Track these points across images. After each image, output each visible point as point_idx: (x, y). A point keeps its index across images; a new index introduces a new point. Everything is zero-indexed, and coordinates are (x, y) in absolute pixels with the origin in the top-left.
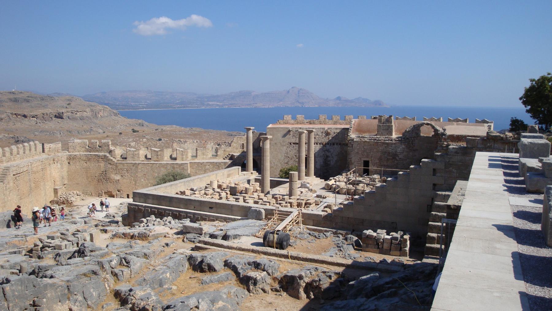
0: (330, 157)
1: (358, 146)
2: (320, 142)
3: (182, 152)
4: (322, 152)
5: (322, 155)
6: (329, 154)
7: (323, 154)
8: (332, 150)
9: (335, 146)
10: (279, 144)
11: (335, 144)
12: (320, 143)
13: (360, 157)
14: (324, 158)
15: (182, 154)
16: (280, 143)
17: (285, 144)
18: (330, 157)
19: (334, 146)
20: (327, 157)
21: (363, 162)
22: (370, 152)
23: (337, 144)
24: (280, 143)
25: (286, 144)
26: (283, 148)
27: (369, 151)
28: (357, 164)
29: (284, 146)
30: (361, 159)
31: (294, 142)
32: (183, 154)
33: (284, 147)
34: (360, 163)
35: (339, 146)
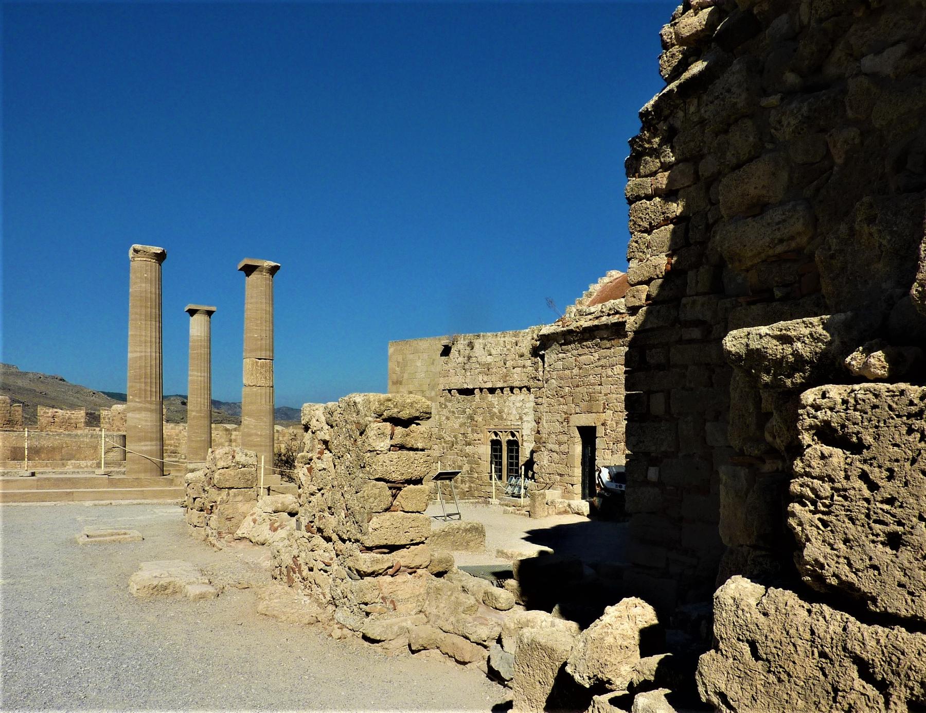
25: (437, 396)
31: (459, 387)
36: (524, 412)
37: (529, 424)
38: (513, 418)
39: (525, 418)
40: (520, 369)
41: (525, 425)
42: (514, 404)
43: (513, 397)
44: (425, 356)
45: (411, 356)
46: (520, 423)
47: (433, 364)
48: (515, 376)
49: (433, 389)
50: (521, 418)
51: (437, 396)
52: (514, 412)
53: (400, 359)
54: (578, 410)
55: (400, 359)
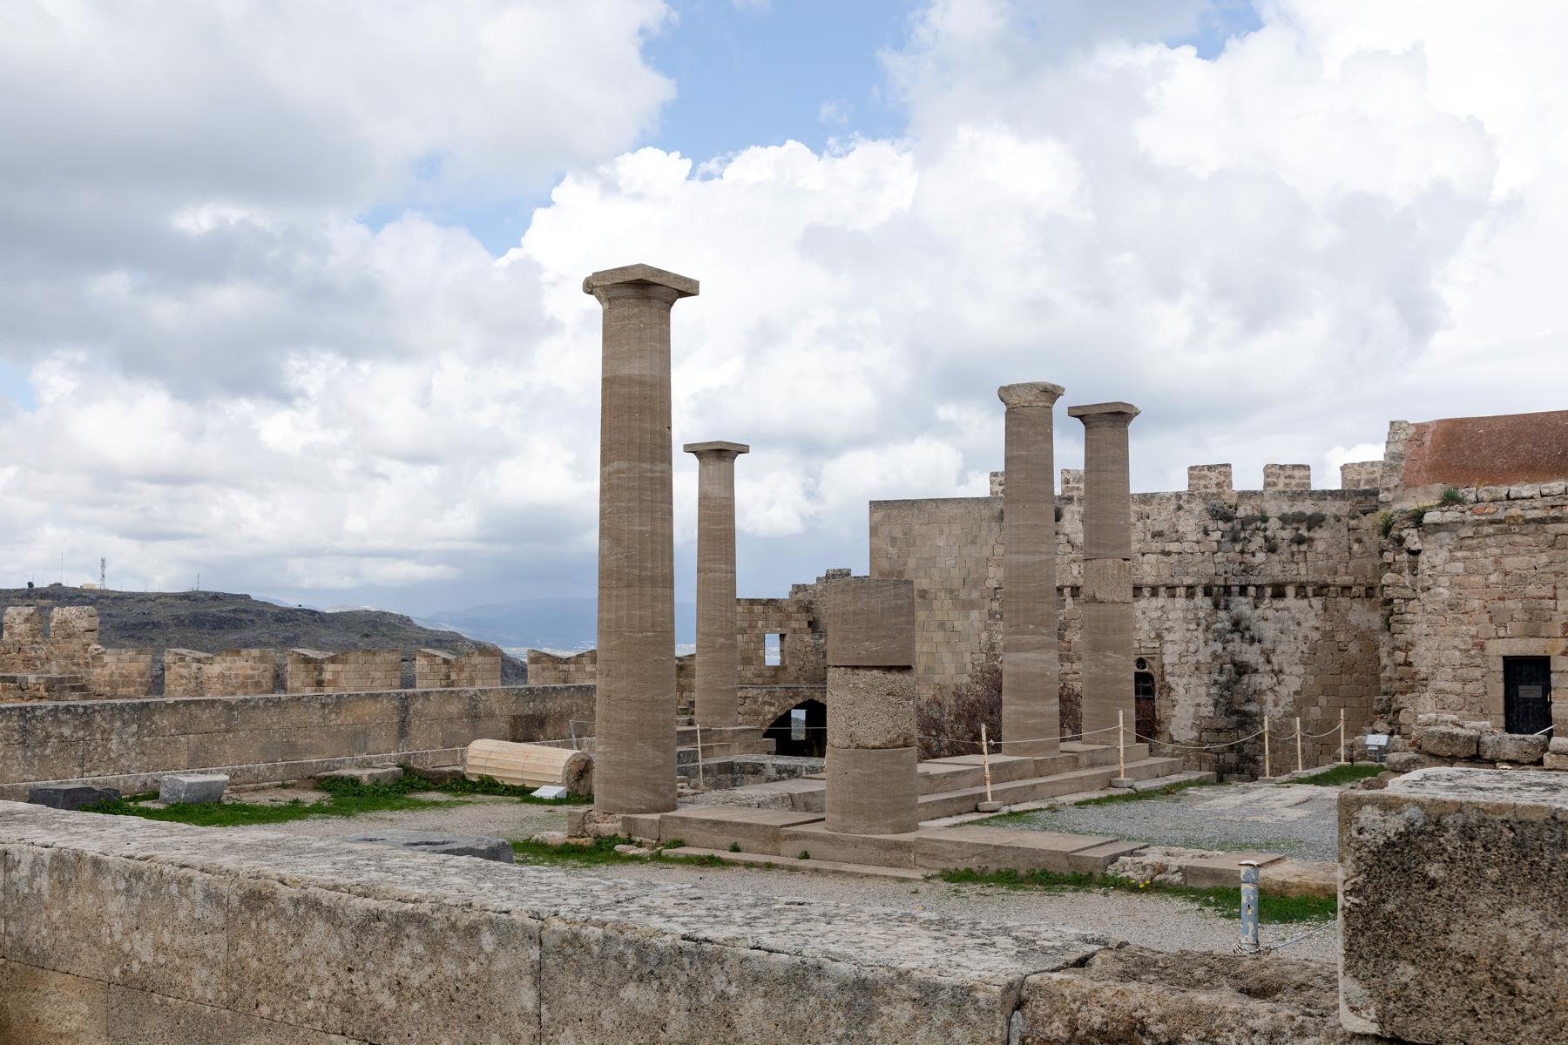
0: (1256, 671)
1: (1453, 559)
2: (1189, 581)
3: (444, 669)
4: (1206, 643)
5: (1204, 656)
6: (1251, 655)
7: (1215, 656)
8: (1268, 631)
9: (1290, 600)
10: (942, 594)
11: (1290, 591)
12: (1189, 587)
13: (1473, 630)
14: (1222, 679)
15: (448, 677)
16: (951, 591)
17: (975, 595)
18: (1256, 671)
19: (1280, 604)
20: (1242, 669)
21: (1499, 666)
22: (1555, 598)
23: (1301, 590)
24: (951, 591)
25: (983, 598)
26: (967, 617)
27: (1548, 591)
28: (1457, 686)
29: (969, 605)
30: (1482, 648)
32: (453, 676)
33: (974, 614)
34: (1478, 673)
35: (1317, 603)
36: (1167, 626)
37: (1176, 647)
38: (1142, 636)
39: (1167, 637)
40: (1155, 556)
41: (1168, 648)
42: (1144, 613)
43: (1142, 603)
44: (956, 529)
45: (925, 529)
46: (1157, 645)
47: (973, 542)
48: (1146, 567)
49: (975, 585)
50: (1159, 637)
51: (983, 598)
52: (1146, 627)
53: (898, 533)
54: (1502, 633)
55: (898, 533)
